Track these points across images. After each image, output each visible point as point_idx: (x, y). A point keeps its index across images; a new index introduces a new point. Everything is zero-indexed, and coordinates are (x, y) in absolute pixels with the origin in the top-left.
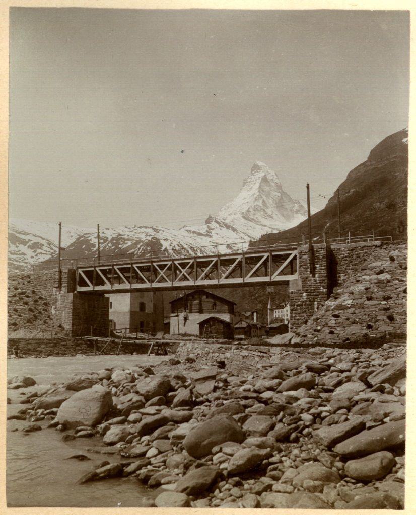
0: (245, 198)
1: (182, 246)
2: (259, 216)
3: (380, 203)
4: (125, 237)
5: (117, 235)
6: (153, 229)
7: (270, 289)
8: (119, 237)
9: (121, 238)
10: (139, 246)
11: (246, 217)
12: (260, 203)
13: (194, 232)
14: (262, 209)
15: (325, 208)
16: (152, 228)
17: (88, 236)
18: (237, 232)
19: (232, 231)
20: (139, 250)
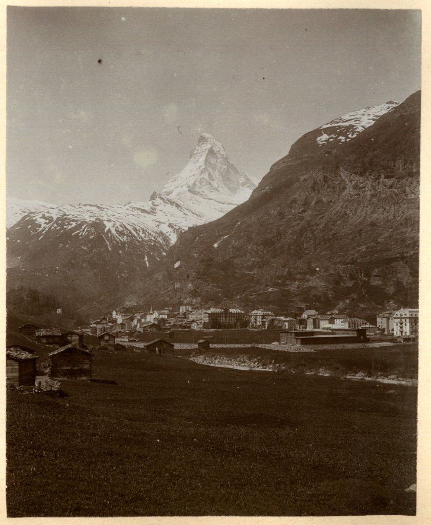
1: (125, 227)
2: (206, 190)
8: (65, 217)
9: (66, 219)
11: (191, 190)
12: (206, 176)
13: (138, 209)
15: (250, 198)
20: (83, 232)
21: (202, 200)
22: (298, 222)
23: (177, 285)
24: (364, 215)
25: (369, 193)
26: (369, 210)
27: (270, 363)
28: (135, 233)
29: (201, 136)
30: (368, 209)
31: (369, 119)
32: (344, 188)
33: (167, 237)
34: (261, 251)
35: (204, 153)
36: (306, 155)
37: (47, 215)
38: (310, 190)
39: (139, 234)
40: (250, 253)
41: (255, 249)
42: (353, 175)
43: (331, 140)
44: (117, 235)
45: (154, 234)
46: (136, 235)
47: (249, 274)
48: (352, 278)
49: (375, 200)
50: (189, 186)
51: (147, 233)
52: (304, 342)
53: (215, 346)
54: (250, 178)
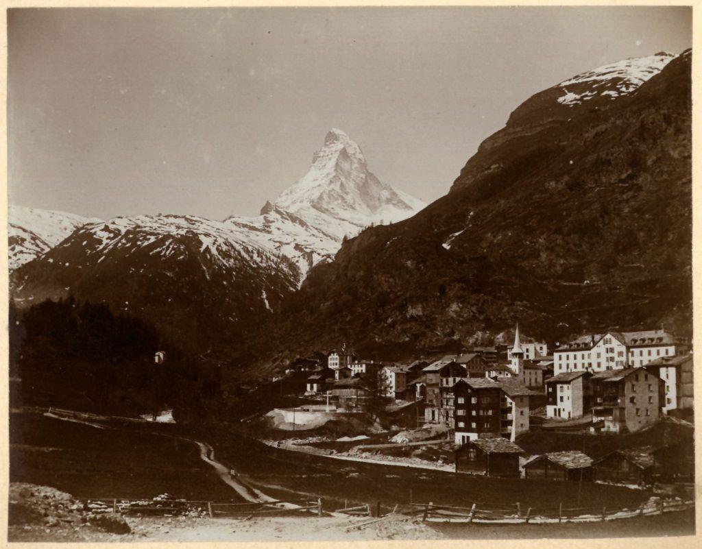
0: (315, 180)
1: (233, 247)
2: (336, 206)
3: (557, 182)
4: (144, 229)
5: (134, 226)
6: (187, 219)
7: (414, 310)
8: (138, 229)
9: (140, 232)
10: (167, 243)
11: (316, 206)
12: (337, 187)
13: (245, 226)
14: (340, 196)
16: (184, 217)
17: (92, 227)
18: (307, 226)
19: (300, 226)
20: (167, 250)
21: (333, 220)
28: (246, 256)
29: (330, 132)
33: (293, 264)
34: (575, 245)
35: (334, 155)
37: (112, 227)
39: (252, 257)
44: (220, 257)
45: (275, 259)
46: (249, 259)
50: (312, 201)
51: (264, 257)
54: (397, 192)
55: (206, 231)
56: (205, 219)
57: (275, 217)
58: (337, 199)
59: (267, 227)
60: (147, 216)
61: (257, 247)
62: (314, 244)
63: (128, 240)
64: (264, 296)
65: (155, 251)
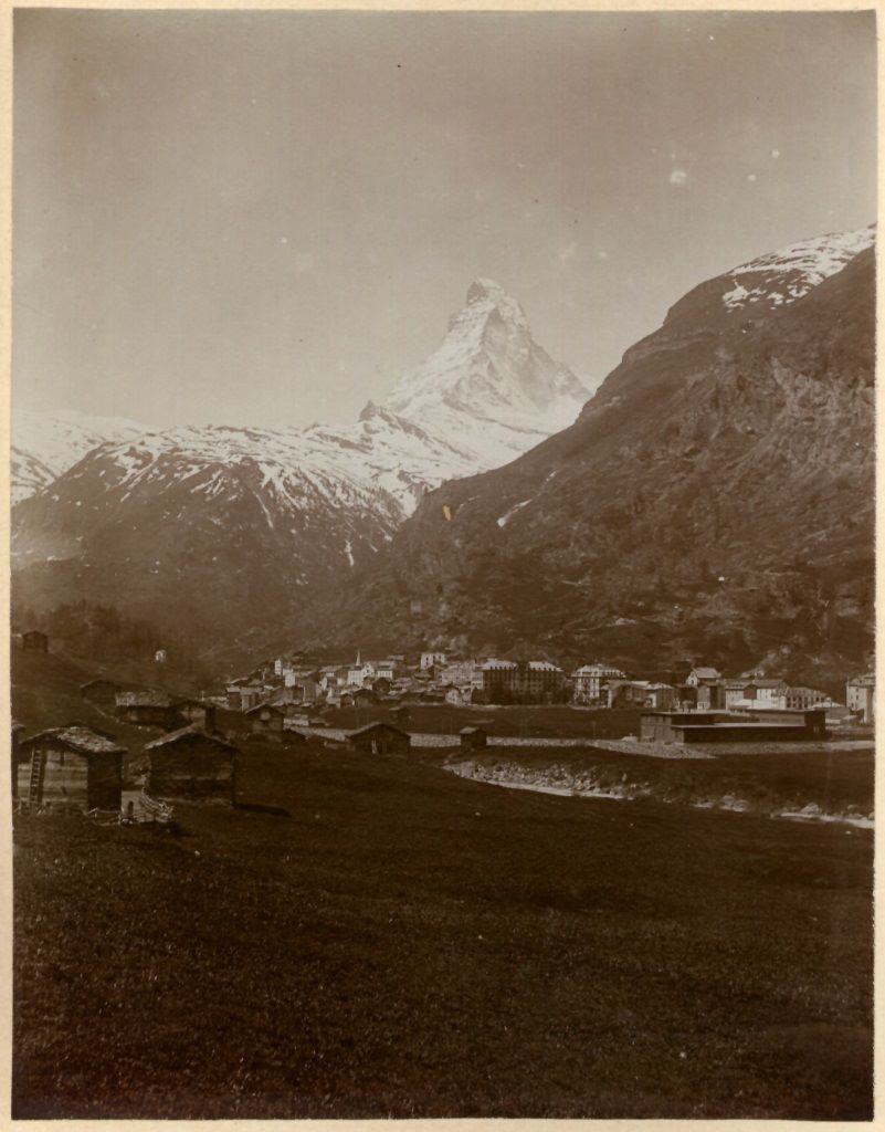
1: (305, 478)
3: (630, 447)
4: (183, 453)
5: (171, 448)
6: (247, 433)
9: (179, 458)
10: (215, 476)
11: (451, 401)
12: (483, 369)
13: (334, 439)
14: (488, 384)
18: (427, 438)
21: (474, 422)
22: (681, 474)
23: (416, 608)
24: (823, 463)
25: (832, 417)
26: (834, 454)
27: (619, 782)
28: (325, 492)
29: (474, 284)
30: (830, 450)
31: (834, 260)
32: (781, 405)
33: (394, 500)
34: (600, 536)
36: (700, 331)
37: (140, 449)
38: (707, 405)
39: (334, 494)
40: (577, 541)
41: (587, 531)
42: (800, 376)
43: (754, 300)
44: (288, 495)
45: (368, 495)
46: (328, 496)
47: (572, 586)
48: (796, 600)
49: (845, 432)
50: (445, 392)
51: (351, 493)
52: (692, 737)
53: (499, 741)
55: (270, 457)
56: (274, 433)
57: (382, 425)
58: (482, 389)
59: (367, 440)
60: (191, 430)
61: (342, 477)
62: (427, 470)
63: (162, 471)
64: (349, 548)
65: (198, 487)
